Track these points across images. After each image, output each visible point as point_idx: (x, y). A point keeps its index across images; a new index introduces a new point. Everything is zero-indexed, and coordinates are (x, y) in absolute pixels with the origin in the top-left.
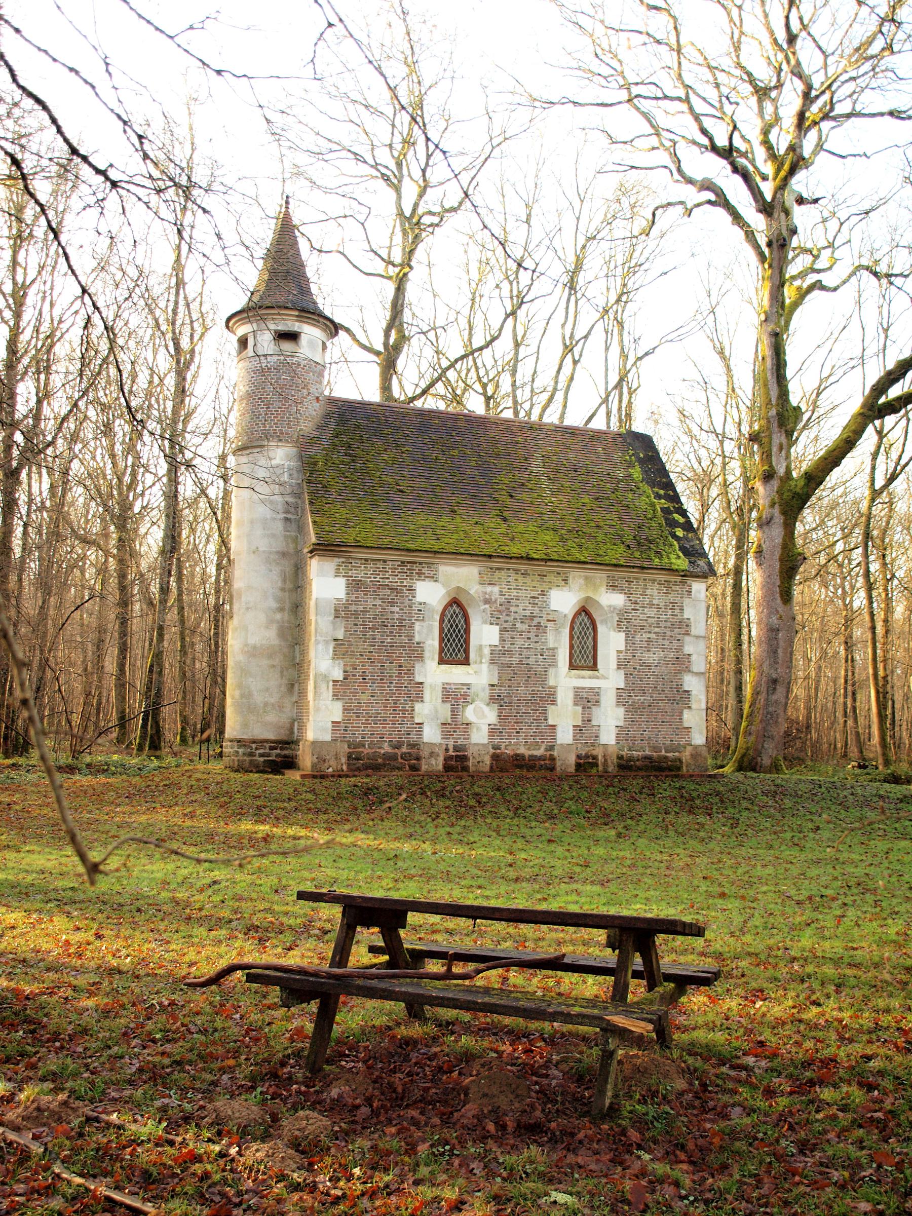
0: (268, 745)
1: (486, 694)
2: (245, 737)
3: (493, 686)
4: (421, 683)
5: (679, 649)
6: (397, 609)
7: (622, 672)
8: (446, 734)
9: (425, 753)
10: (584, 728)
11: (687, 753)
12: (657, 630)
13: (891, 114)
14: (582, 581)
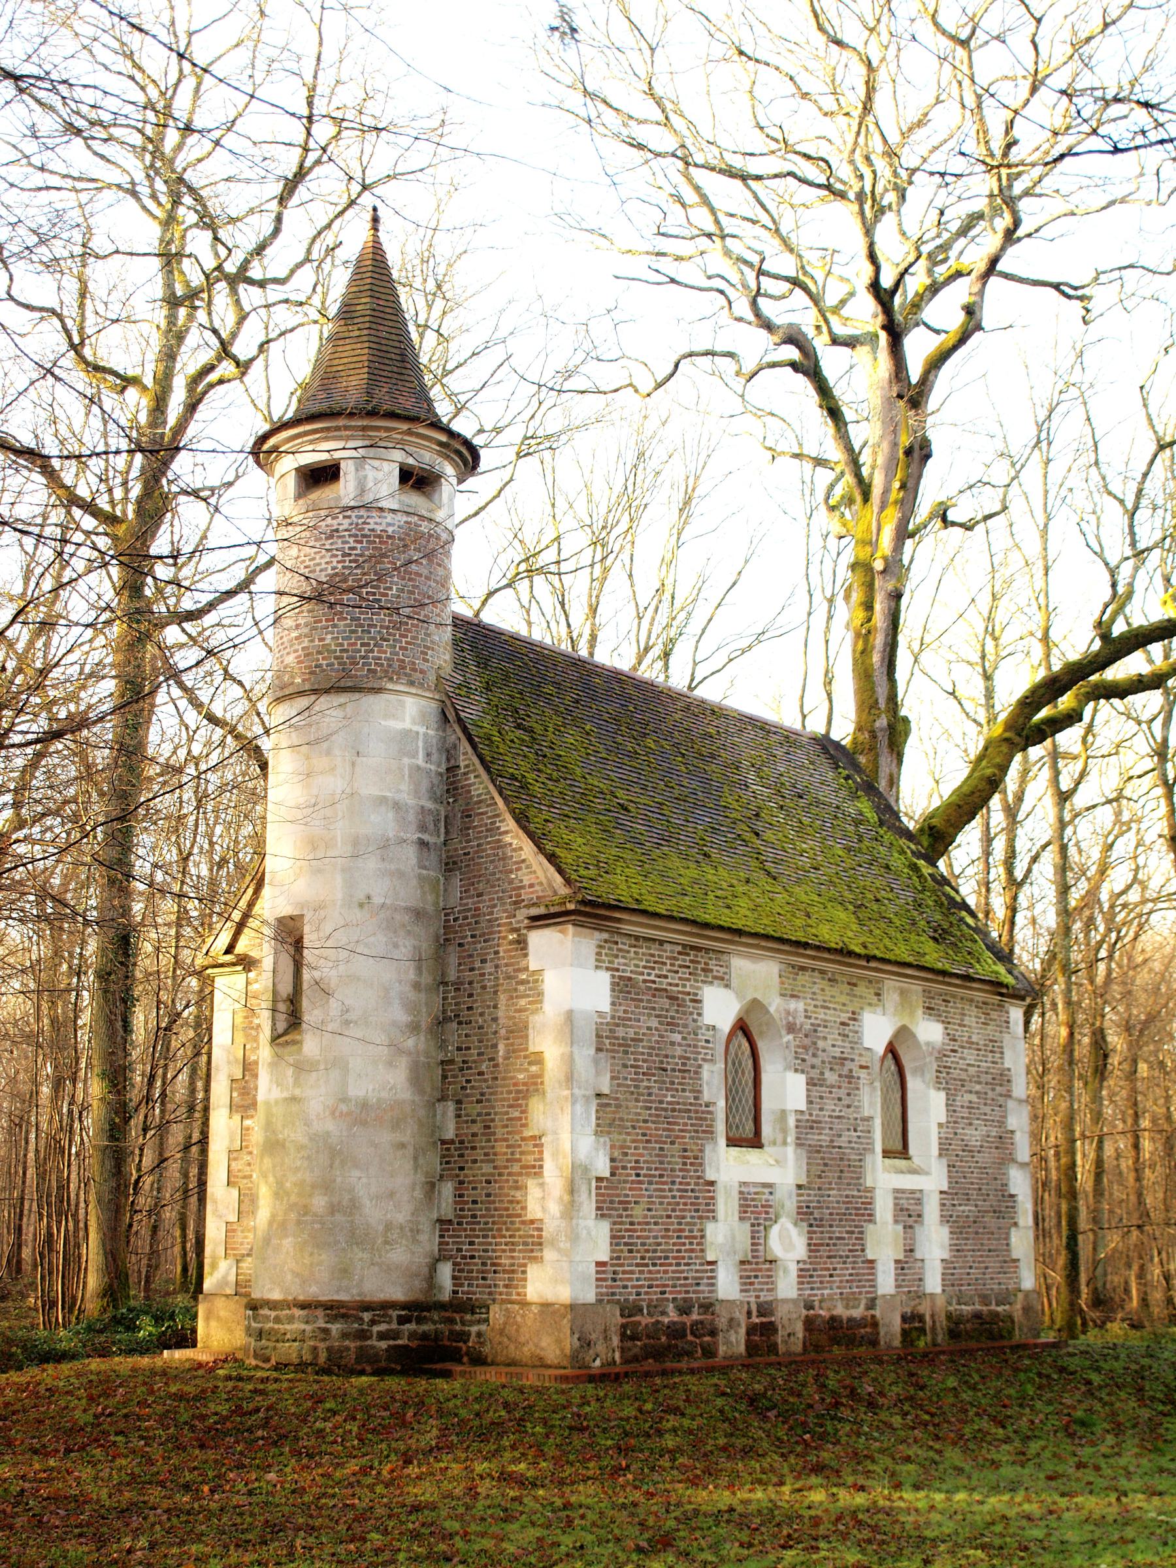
0: (394, 1314)
1: (791, 1205)
2: (343, 1297)
3: (799, 1187)
4: (712, 1183)
5: (1002, 1123)
6: (677, 1037)
7: (944, 1161)
8: (746, 1282)
9: (722, 1323)
10: (907, 1264)
11: (1019, 1306)
12: (978, 1087)
13: (1057, 287)
14: (896, 997)
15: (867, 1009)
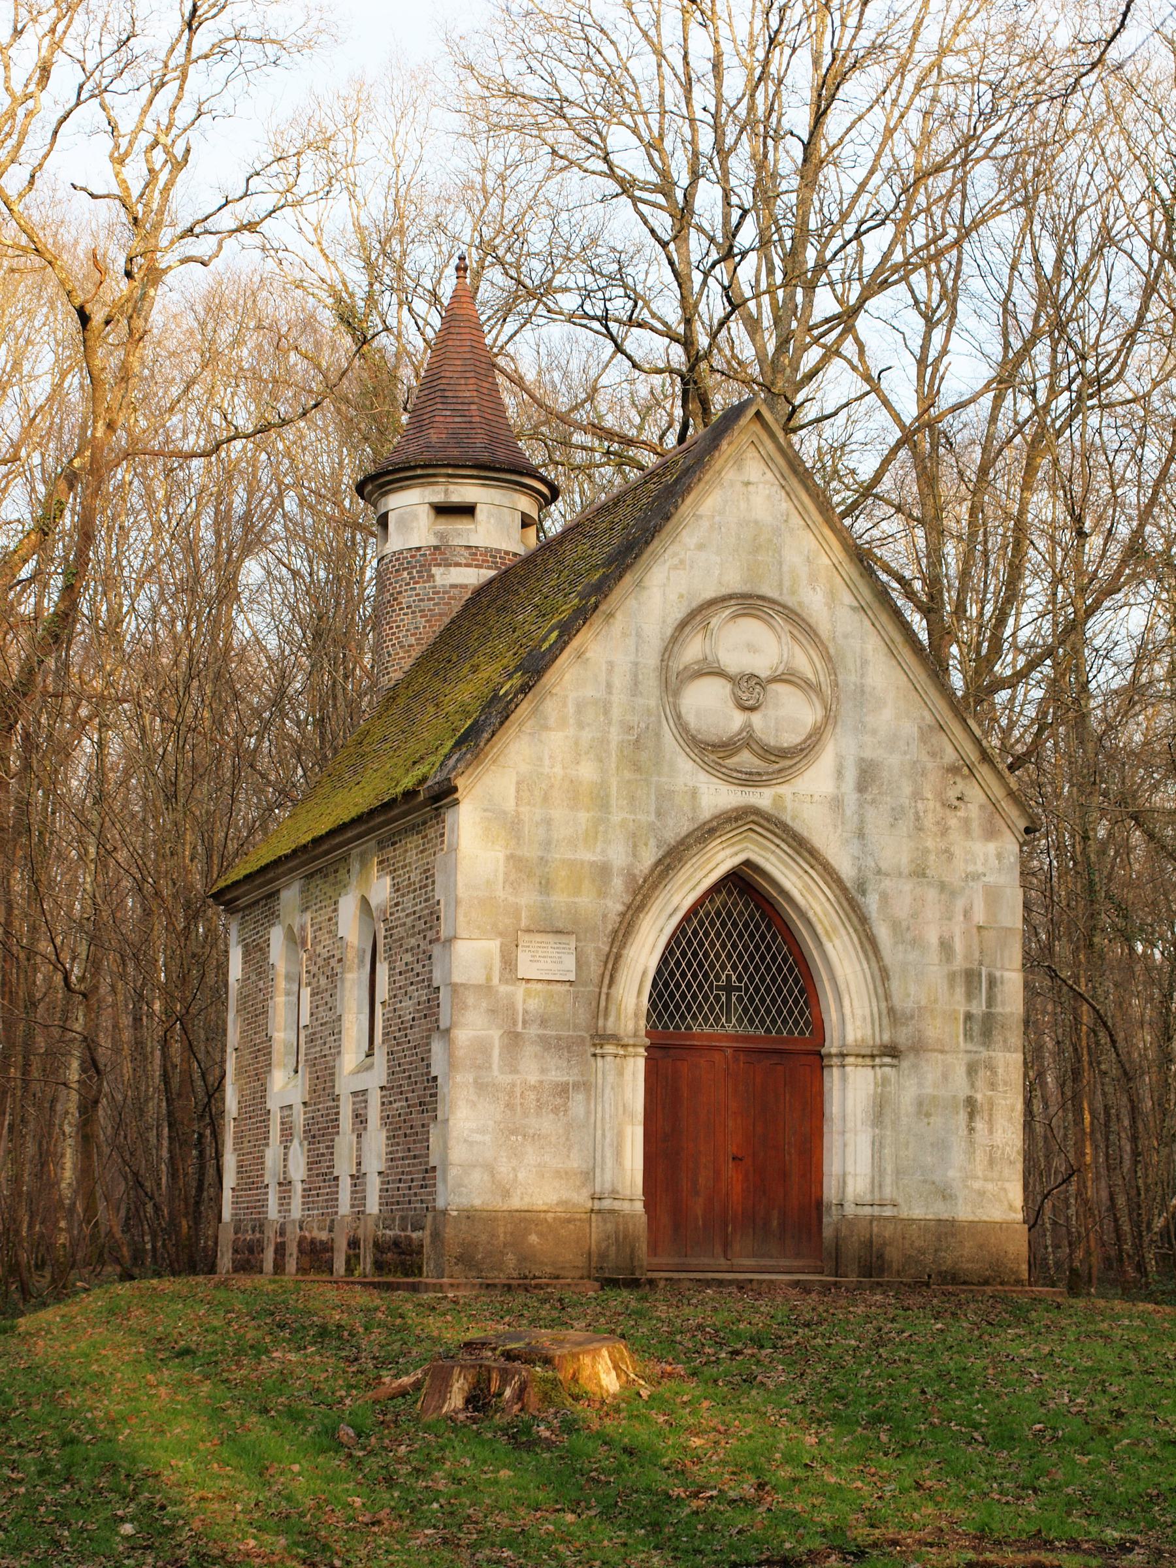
11: (428, 1232)
12: (413, 942)
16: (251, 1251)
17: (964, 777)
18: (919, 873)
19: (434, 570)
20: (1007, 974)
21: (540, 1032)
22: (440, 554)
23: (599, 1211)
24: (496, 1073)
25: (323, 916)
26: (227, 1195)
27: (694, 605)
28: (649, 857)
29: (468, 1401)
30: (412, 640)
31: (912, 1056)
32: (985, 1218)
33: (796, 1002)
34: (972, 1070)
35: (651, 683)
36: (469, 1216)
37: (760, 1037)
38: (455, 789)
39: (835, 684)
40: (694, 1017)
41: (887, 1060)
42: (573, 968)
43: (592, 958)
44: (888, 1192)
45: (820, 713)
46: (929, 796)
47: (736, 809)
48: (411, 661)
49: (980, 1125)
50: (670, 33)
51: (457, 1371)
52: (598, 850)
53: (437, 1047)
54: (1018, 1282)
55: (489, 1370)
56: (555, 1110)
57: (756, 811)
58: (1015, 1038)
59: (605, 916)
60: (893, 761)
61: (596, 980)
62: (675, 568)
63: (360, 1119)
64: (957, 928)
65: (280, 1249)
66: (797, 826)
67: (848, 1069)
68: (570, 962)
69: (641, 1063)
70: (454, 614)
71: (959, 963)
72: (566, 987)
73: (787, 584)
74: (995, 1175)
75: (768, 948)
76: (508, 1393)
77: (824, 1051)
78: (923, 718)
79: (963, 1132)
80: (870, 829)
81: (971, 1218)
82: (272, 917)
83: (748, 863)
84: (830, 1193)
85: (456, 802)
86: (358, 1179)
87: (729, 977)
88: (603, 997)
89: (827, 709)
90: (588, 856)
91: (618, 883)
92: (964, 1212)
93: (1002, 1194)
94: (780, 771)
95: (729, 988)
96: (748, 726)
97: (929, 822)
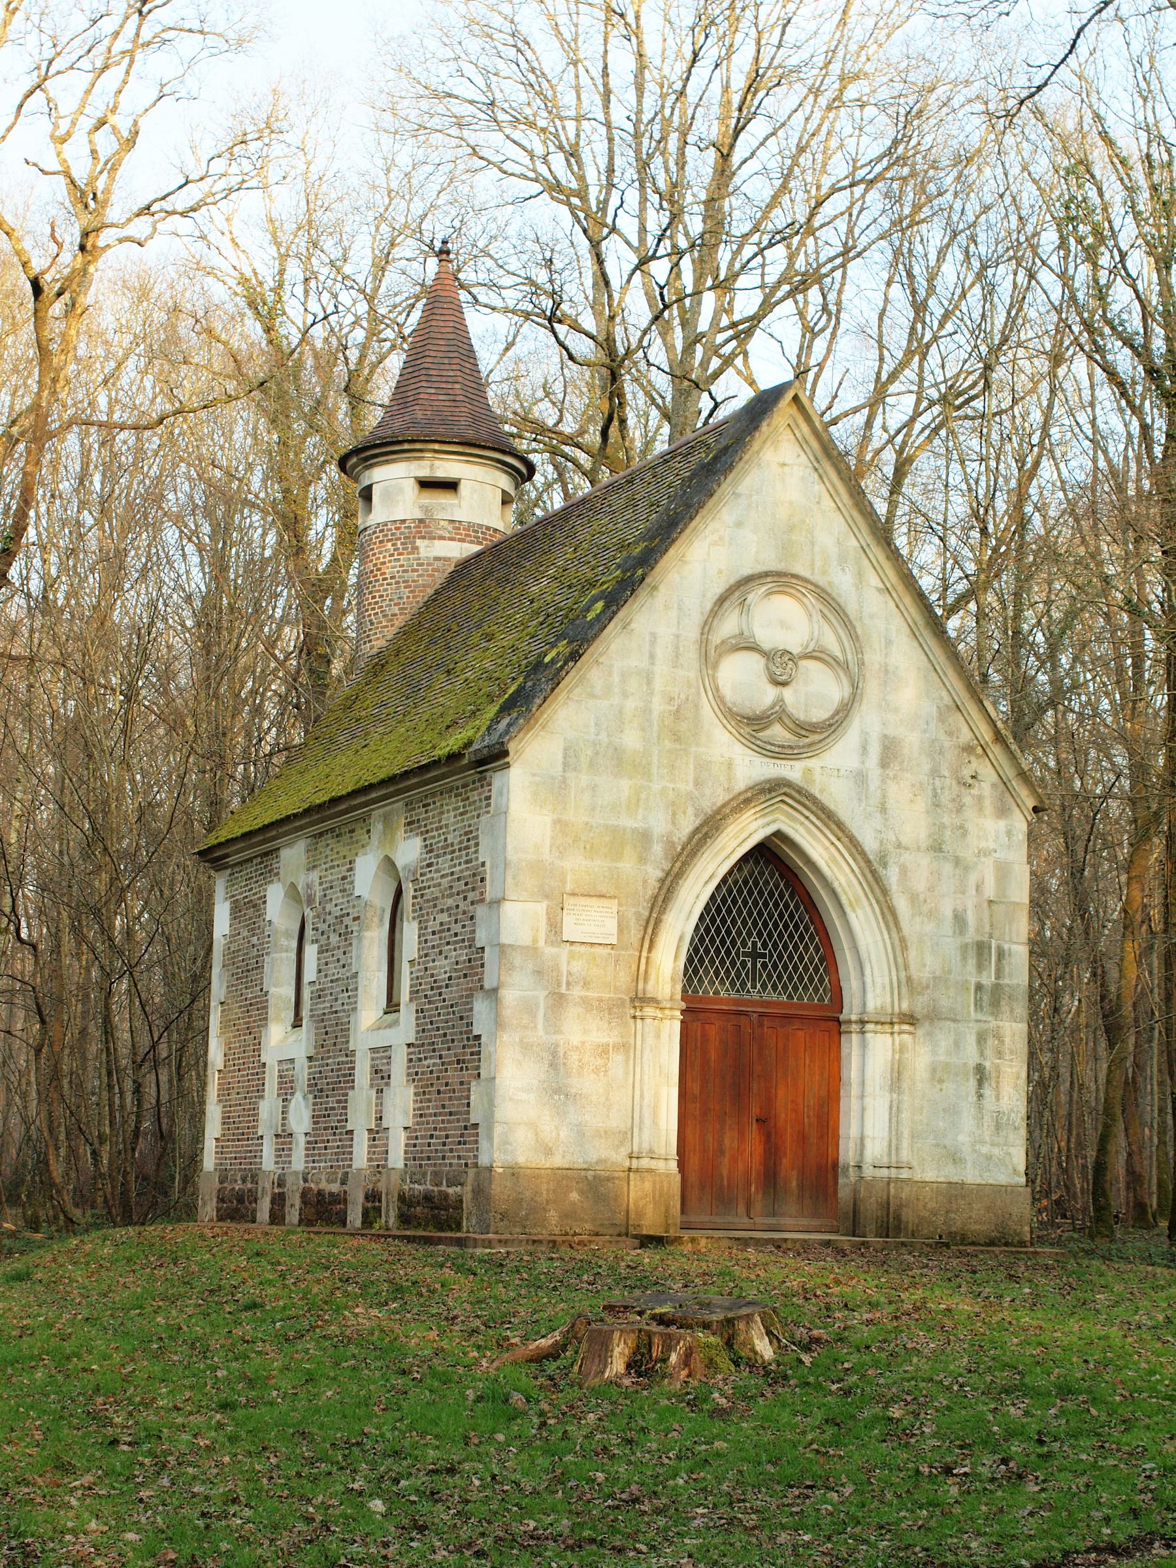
6: (254, 940)
7: (413, 1007)
11: (468, 1188)
12: (450, 902)
15: (361, 852)
16: (241, 1200)
17: (978, 757)
18: (937, 848)
19: (419, 542)
20: (1014, 947)
21: (583, 993)
22: (423, 527)
23: (637, 1170)
24: (541, 1032)
25: (334, 876)
26: (210, 1145)
27: (732, 581)
28: (688, 824)
29: (629, 1366)
30: (396, 610)
31: (927, 1024)
32: (991, 1181)
33: (816, 969)
34: (981, 1039)
35: (691, 655)
36: (514, 1172)
37: (778, 1004)
38: (506, 753)
39: (861, 663)
40: (722, 982)
41: (906, 1027)
42: (615, 931)
43: (633, 923)
44: (905, 1155)
45: (847, 691)
46: (946, 774)
47: (768, 781)
48: (394, 630)
49: (987, 1092)
50: (590, 49)
51: (616, 1335)
52: (640, 817)
53: (480, 1008)
54: (1022, 1244)
55: (650, 1335)
56: (596, 1071)
57: (788, 784)
58: (1021, 1009)
59: (645, 881)
60: (912, 741)
61: (637, 944)
62: (715, 544)
63: (381, 1076)
64: (970, 903)
65: (279, 1200)
66: (825, 799)
67: (868, 1035)
68: (612, 925)
69: (677, 1025)
70: (437, 586)
71: (971, 936)
72: (608, 950)
73: (818, 564)
74: (1001, 1140)
75: (791, 916)
76: (673, 1358)
77: (842, 1017)
78: (942, 699)
79: (973, 1098)
80: (891, 803)
81: (979, 1181)
82: (270, 874)
83: (778, 834)
84: (847, 1153)
85: (507, 766)
86: (378, 1133)
87: (754, 943)
88: (643, 961)
89: (855, 686)
90: (628, 822)
91: (658, 849)
92: (971, 1176)
93: (1007, 1158)
94: (810, 745)
95: (755, 955)
96: (780, 701)
97: (945, 798)
